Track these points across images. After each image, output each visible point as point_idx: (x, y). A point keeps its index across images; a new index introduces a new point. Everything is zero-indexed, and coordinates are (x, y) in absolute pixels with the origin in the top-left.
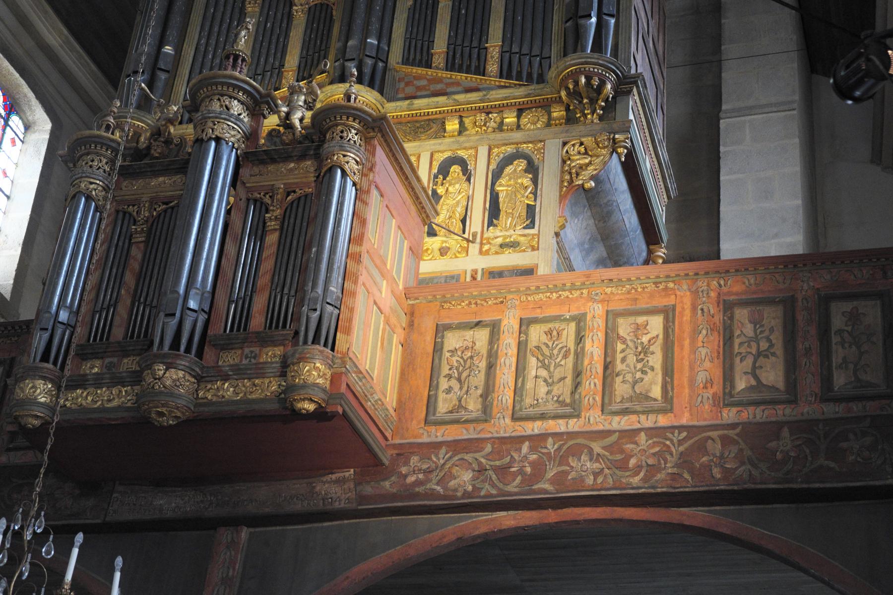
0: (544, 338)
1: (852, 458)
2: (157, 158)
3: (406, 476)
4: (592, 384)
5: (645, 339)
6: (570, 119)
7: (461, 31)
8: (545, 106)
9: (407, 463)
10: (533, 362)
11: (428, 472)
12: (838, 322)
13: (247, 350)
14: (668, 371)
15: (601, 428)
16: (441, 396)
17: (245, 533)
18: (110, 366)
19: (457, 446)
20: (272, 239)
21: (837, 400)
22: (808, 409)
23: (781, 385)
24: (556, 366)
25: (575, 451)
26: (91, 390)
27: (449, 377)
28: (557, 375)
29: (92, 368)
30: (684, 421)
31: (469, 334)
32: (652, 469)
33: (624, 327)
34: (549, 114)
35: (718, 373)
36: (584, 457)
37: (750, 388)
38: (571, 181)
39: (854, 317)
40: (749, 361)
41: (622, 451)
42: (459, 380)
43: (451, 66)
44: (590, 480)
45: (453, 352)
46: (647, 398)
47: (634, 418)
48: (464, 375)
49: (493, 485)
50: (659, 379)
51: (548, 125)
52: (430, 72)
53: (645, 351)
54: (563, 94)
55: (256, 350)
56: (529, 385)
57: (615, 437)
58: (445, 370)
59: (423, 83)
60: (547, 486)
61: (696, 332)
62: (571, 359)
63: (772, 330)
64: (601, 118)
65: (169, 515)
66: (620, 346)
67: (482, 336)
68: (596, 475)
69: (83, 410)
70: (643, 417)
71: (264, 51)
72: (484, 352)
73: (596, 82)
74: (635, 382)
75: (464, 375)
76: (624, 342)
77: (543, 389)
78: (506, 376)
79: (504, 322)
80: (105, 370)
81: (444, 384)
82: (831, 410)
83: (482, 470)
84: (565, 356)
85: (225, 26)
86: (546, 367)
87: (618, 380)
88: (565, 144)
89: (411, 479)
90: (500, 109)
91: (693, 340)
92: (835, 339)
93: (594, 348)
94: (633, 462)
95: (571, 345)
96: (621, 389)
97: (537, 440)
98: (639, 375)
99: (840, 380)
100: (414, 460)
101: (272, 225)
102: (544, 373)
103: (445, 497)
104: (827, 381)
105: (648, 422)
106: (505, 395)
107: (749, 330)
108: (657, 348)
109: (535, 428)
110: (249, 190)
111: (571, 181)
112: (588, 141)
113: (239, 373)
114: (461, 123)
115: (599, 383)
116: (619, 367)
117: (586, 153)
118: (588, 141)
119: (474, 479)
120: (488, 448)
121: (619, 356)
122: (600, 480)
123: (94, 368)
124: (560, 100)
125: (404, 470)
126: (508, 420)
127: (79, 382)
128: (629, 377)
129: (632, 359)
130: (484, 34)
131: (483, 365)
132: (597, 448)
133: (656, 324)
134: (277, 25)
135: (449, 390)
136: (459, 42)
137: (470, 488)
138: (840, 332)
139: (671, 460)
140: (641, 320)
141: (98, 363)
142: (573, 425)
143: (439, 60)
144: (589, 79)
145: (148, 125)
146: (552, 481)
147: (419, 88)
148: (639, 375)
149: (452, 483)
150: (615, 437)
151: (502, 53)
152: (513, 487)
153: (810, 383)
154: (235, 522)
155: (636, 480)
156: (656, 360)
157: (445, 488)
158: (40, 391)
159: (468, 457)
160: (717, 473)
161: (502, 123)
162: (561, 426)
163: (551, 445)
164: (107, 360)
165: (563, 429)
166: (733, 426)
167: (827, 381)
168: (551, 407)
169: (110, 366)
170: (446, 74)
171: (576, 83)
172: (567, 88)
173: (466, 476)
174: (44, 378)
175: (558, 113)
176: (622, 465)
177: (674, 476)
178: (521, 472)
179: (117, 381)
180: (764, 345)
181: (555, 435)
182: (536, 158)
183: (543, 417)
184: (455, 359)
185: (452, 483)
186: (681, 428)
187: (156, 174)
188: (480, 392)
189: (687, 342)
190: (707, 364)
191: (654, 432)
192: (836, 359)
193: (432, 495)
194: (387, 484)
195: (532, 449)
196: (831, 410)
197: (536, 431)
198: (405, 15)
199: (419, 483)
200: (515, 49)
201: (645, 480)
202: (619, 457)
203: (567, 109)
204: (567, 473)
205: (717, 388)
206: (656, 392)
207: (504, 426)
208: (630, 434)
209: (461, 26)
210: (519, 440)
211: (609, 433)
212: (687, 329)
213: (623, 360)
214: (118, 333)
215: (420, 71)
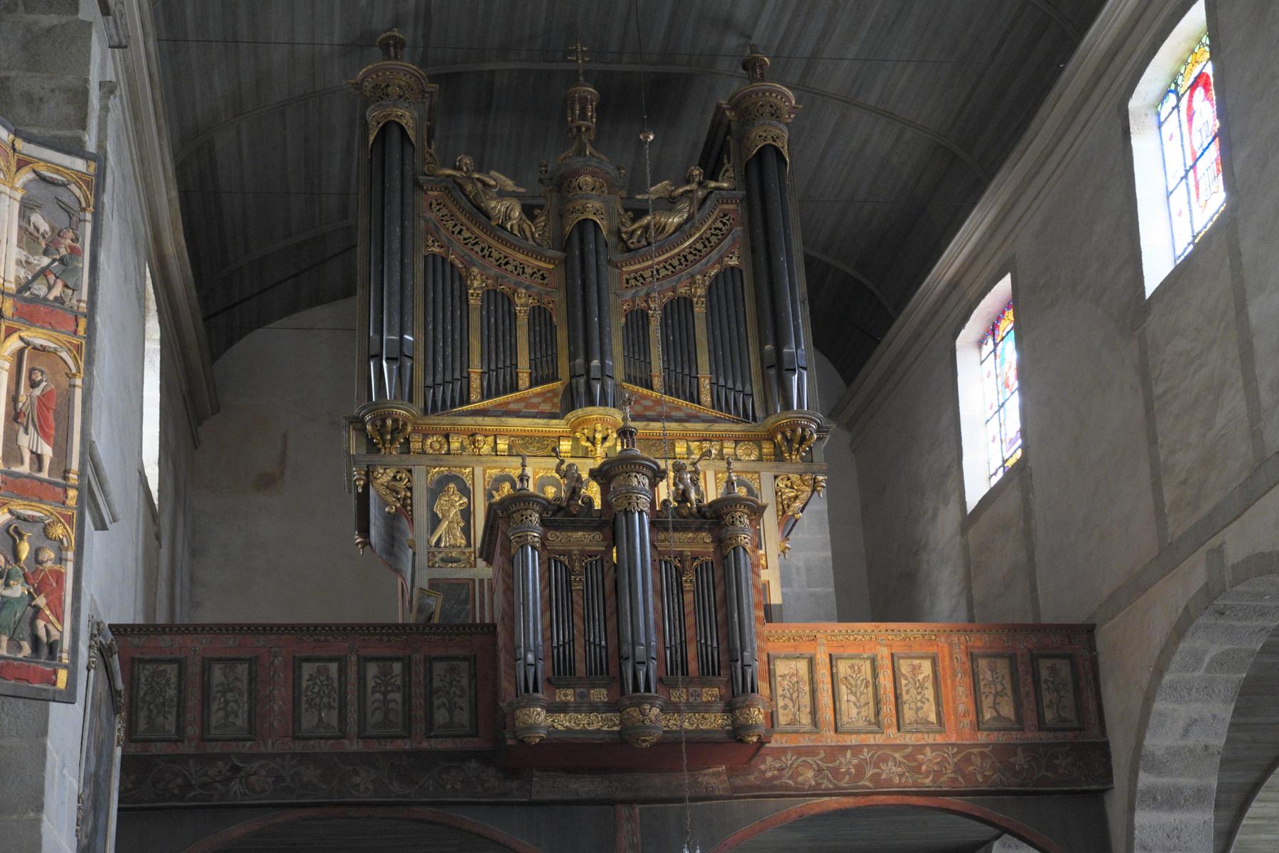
0: (849, 671)
1: (1061, 771)
2: (574, 516)
3: (764, 772)
4: (888, 708)
5: (920, 677)
6: (778, 456)
7: (672, 357)
8: (757, 441)
9: (764, 762)
10: (843, 689)
11: (781, 769)
12: (1044, 674)
13: (691, 690)
14: (938, 704)
15: (899, 742)
16: (781, 711)
17: (637, 808)
18: (582, 696)
19: (799, 751)
20: (689, 598)
21: (1049, 730)
22: (1031, 736)
23: (1012, 717)
24: (862, 693)
25: (885, 759)
26: (573, 715)
27: (784, 696)
28: (863, 701)
29: (566, 695)
30: (953, 740)
31: (792, 663)
32: (938, 774)
33: (904, 667)
34: (760, 448)
35: (972, 707)
36: (890, 764)
37: (993, 718)
38: (784, 512)
39: (1053, 670)
40: (991, 697)
41: (915, 760)
42: (791, 699)
43: (668, 391)
44: (897, 780)
45: (783, 676)
46: (928, 723)
47: (920, 735)
48: (795, 696)
49: (830, 781)
50: (933, 708)
51: (760, 459)
52: (654, 394)
53: (922, 686)
54: (779, 437)
55: (699, 690)
56: (844, 707)
57: (910, 749)
58: (780, 691)
59: (649, 403)
60: (867, 783)
61: (954, 675)
62: (870, 689)
63: (1003, 677)
64: (802, 458)
65: (585, 796)
66: (904, 682)
67: (803, 666)
68: (901, 776)
69: (568, 730)
70: (926, 736)
71: (493, 346)
72: (806, 678)
73: (808, 433)
74: (918, 709)
75: (795, 696)
76: (906, 678)
77: (854, 711)
78: (825, 699)
79: (818, 656)
80: (578, 699)
81: (781, 703)
82: (1046, 737)
83: (820, 770)
84: (867, 687)
85: (449, 315)
86: (854, 694)
87: (906, 707)
88: (776, 477)
89: (769, 774)
90: (721, 439)
91: (953, 681)
92: (1044, 686)
93: (886, 681)
94: (924, 768)
95: (869, 678)
96: (908, 714)
97: (856, 749)
98: (919, 704)
99: (1049, 715)
100: (769, 759)
101: (687, 586)
102: (852, 698)
103: (796, 789)
104: (1040, 716)
105: (930, 739)
106: (827, 714)
107: (989, 675)
108: (929, 684)
109: (853, 740)
110: (660, 553)
111: (784, 512)
112: (794, 477)
113: (693, 708)
114: (688, 448)
115: (893, 708)
116: (905, 697)
117: (792, 487)
118: (794, 477)
119: (815, 776)
120: (822, 754)
121: (904, 689)
122: (903, 780)
123: (568, 695)
124: (771, 438)
125: (762, 767)
126: (832, 733)
127: (563, 708)
128: (913, 705)
129: (913, 692)
130: (692, 361)
131: (807, 688)
132: (897, 755)
133: (926, 666)
134: (500, 321)
135: (785, 707)
136: (672, 367)
137: (813, 783)
138: (1046, 681)
139: (950, 769)
140: (916, 662)
141: (570, 692)
142: (879, 739)
143: (657, 382)
144: (803, 430)
145: (413, 415)
146: (870, 780)
147: (646, 408)
148: (919, 704)
149: (800, 779)
150: (910, 749)
151: (711, 384)
152: (843, 784)
153: (1031, 718)
154: (630, 802)
155: (928, 781)
156: (929, 693)
157: (796, 782)
158: (539, 716)
159: (809, 760)
160: (979, 777)
161: (721, 450)
162: (871, 739)
163: (866, 754)
164: (578, 690)
165: (872, 742)
166: (986, 745)
167: (1040, 716)
168: (861, 724)
169: (582, 696)
170: (667, 398)
171: (794, 431)
172: (783, 434)
173: (810, 774)
174: (542, 707)
175: (767, 448)
176: (917, 770)
177: (953, 780)
178: (848, 772)
179: (593, 708)
180: (999, 688)
181: (868, 746)
182: (755, 486)
183: (858, 732)
184: (785, 682)
185: (800, 779)
186: (953, 745)
187: (576, 529)
188: (808, 710)
189: (949, 682)
190: (964, 699)
191: (935, 747)
192: (1046, 701)
193: (787, 787)
194: (752, 778)
195: (853, 755)
196: (1046, 737)
197: (854, 743)
198: (620, 333)
199: (774, 778)
200: (722, 382)
201: (934, 781)
202: (914, 764)
203: (776, 446)
204: (880, 775)
205: (972, 717)
206: (933, 717)
207: (829, 738)
208: (920, 748)
209: (671, 352)
210: (843, 748)
211: (906, 746)
212: (948, 672)
213: (908, 692)
214: (581, 668)
215: (645, 391)
